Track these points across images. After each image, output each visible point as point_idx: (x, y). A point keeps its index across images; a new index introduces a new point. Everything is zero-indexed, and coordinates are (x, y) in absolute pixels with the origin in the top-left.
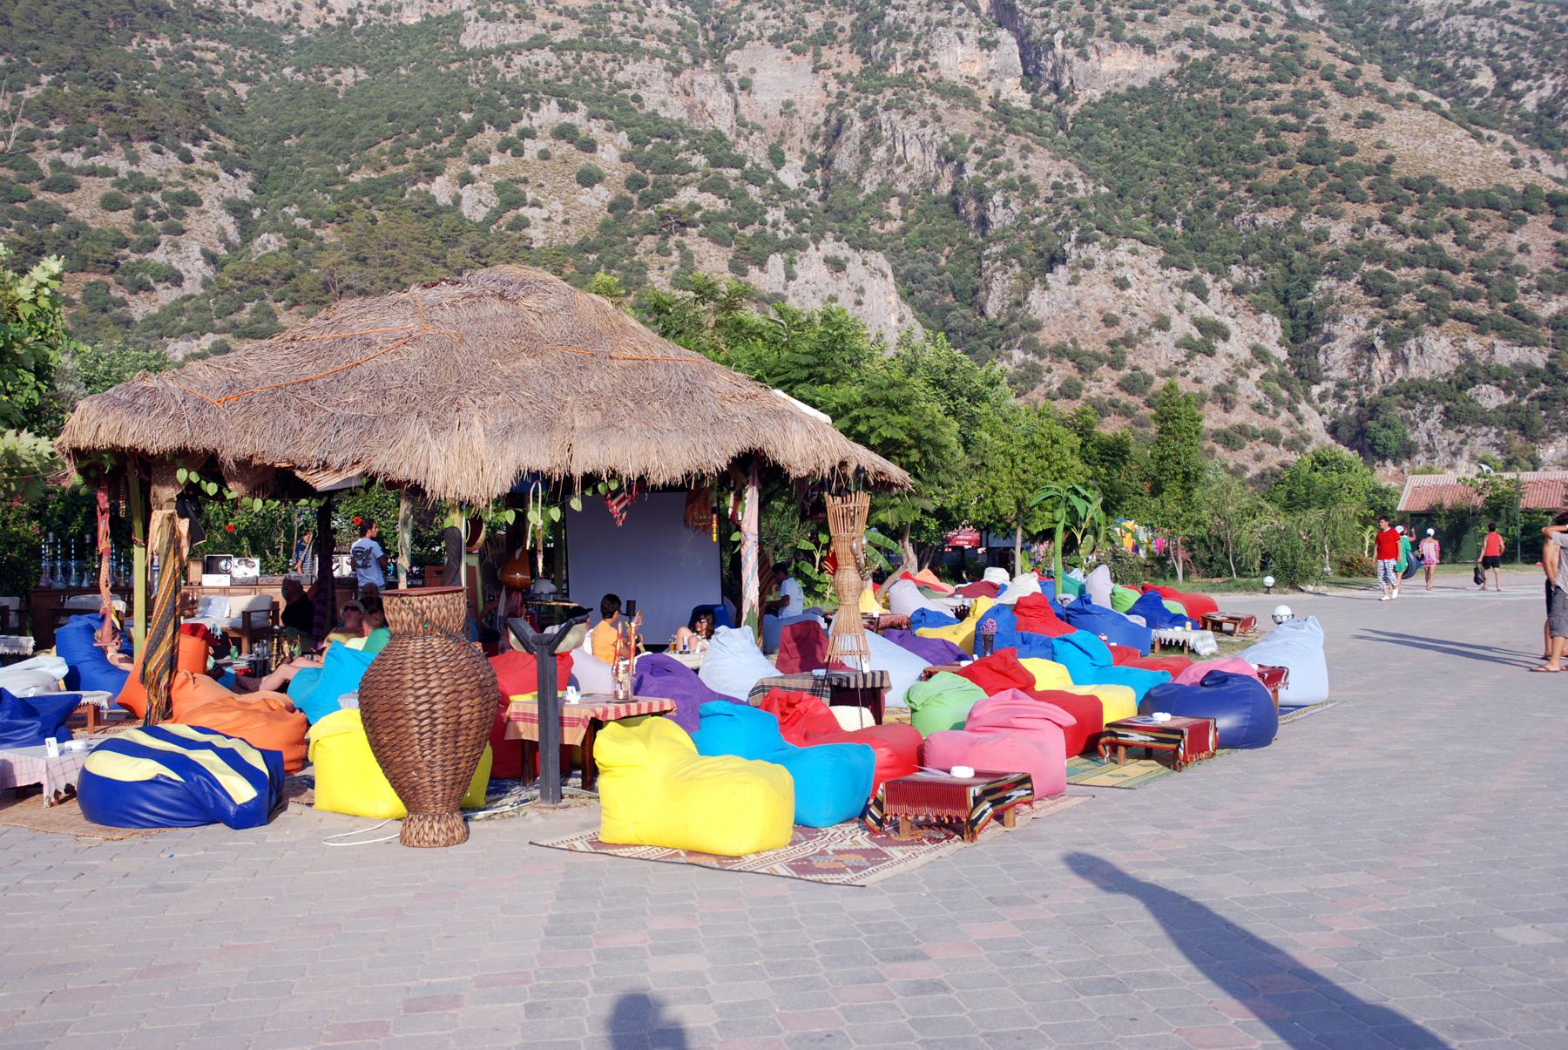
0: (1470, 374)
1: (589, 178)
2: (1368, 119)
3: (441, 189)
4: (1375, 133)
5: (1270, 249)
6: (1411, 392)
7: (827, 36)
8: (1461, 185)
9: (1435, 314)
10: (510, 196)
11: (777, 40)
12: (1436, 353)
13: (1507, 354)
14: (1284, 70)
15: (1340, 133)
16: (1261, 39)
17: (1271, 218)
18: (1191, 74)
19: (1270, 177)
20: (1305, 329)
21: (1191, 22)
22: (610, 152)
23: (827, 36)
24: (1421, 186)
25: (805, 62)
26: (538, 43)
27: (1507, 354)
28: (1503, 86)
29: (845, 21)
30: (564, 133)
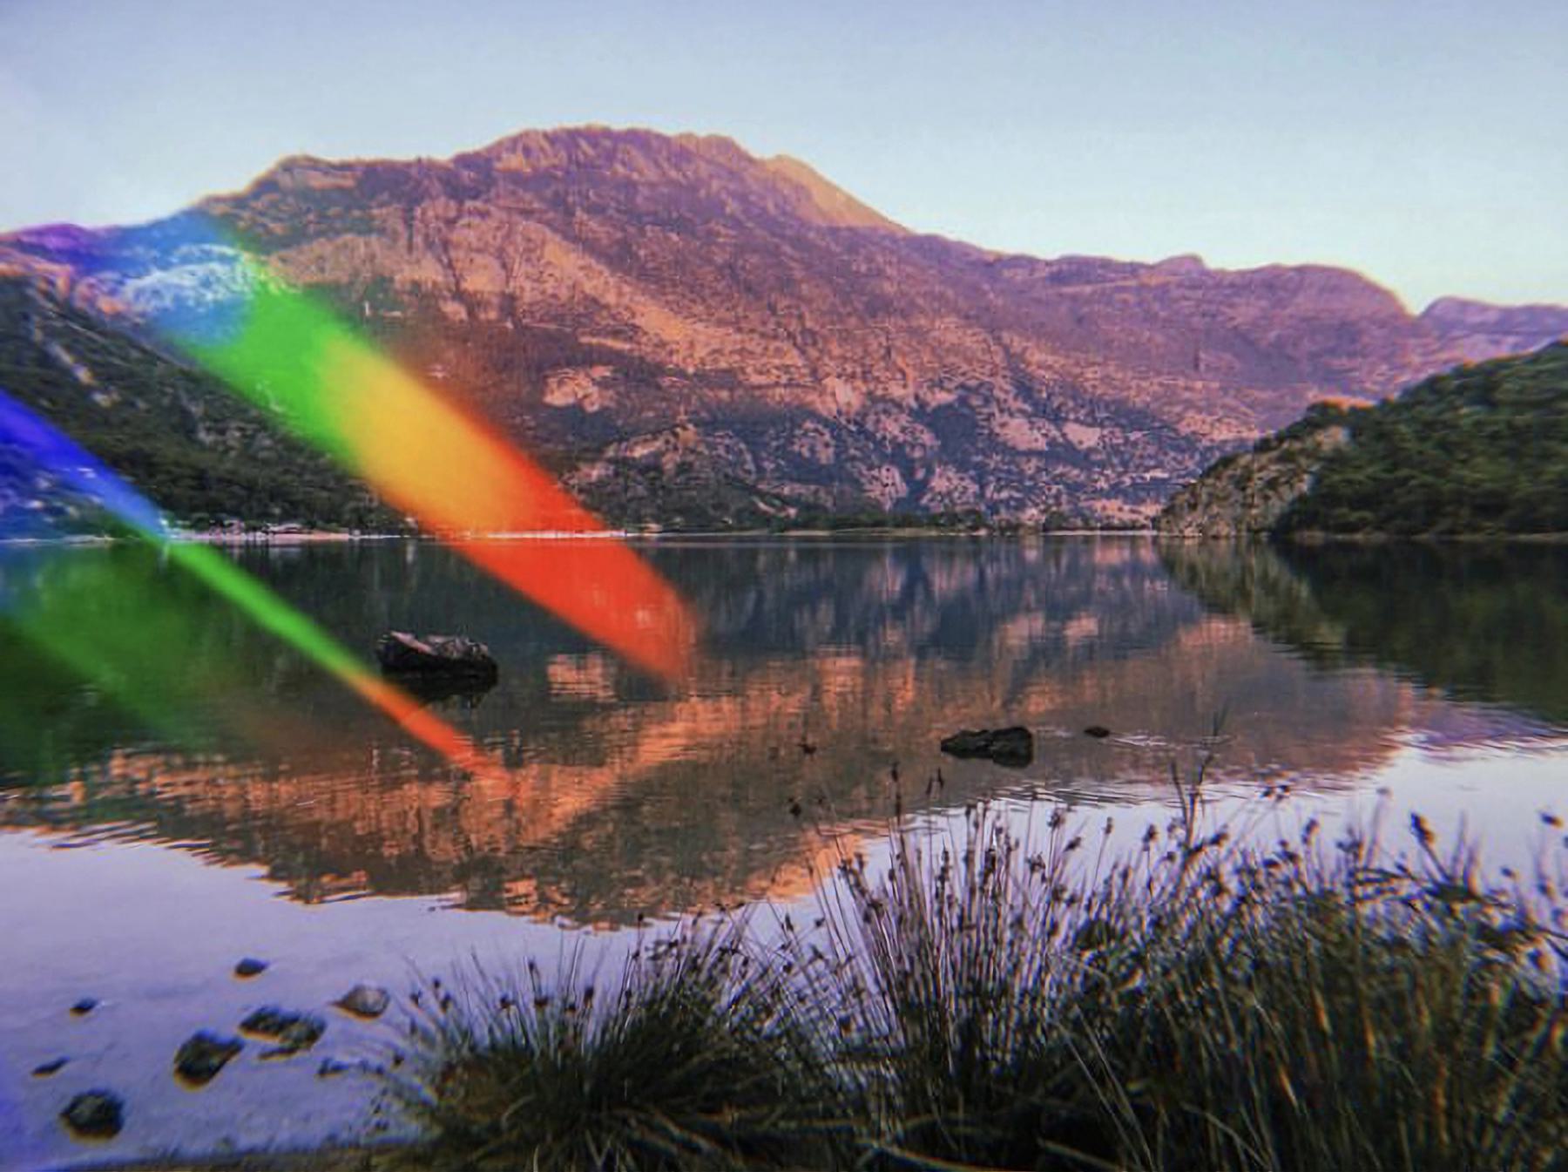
0: (1011, 498)
1: (827, 445)
2: (1003, 425)
3: (796, 448)
4: (1005, 431)
5: (977, 466)
6: (1001, 501)
7: (853, 376)
8: (1023, 447)
9: (1006, 486)
10: (812, 450)
11: (839, 376)
12: (1004, 494)
13: (1017, 495)
14: (987, 401)
15: (997, 430)
16: (981, 385)
17: (979, 458)
18: (963, 401)
19: (980, 445)
20: (983, 487)
21: (962, 379)
22: (827, 437)
23: (853, 376)
24: (1013, 448)
25: (849, 387)
26: (777, 384)
27: (1017, 495)
28: (1049, 396)
29: (859, 370)
30: (816, 430)
